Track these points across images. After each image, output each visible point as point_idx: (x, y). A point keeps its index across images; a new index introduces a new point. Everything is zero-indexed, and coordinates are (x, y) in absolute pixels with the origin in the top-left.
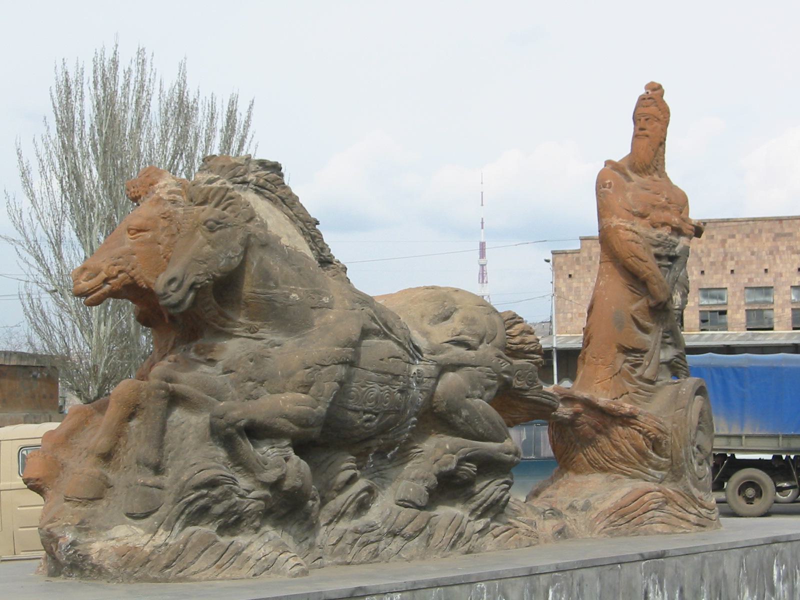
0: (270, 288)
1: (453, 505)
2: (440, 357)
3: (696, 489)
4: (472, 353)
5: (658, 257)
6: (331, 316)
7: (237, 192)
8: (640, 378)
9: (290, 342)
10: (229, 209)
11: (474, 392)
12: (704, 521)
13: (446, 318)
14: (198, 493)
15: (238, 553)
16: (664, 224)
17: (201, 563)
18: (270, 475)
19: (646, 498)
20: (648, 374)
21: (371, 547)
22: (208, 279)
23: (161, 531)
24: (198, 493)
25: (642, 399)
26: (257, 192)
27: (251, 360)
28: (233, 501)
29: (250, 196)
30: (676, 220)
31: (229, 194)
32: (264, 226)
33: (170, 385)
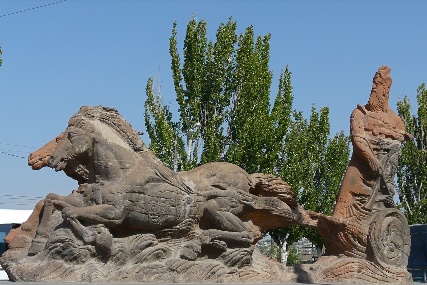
0: (99, 160)
2: (204, 192)
3: (384, 263)
4: (223, 191)
5: (375, 149)
6: (130, 172)
7: (88, 121)
8: (363, 208)
9: (106, 183)
10: (82, 128)
11: (222, 208)
12: (389, 280)
13: (214, 175)
14: (54, 245)
15: (71, 271)
16: (380, 134)
17: (54, 275)
18: (89, 238)
19: (349, 265)
20: (367, 206)
21: (157, 275)
22: (72, 157)
23: (38, 260)
24: (54, 245)
25: (363, 219)
28: (71, 249)
29: (97, 124)
30: (388, 132)
31: (83, 121)
32: (99, 134)
33: (53, 201)
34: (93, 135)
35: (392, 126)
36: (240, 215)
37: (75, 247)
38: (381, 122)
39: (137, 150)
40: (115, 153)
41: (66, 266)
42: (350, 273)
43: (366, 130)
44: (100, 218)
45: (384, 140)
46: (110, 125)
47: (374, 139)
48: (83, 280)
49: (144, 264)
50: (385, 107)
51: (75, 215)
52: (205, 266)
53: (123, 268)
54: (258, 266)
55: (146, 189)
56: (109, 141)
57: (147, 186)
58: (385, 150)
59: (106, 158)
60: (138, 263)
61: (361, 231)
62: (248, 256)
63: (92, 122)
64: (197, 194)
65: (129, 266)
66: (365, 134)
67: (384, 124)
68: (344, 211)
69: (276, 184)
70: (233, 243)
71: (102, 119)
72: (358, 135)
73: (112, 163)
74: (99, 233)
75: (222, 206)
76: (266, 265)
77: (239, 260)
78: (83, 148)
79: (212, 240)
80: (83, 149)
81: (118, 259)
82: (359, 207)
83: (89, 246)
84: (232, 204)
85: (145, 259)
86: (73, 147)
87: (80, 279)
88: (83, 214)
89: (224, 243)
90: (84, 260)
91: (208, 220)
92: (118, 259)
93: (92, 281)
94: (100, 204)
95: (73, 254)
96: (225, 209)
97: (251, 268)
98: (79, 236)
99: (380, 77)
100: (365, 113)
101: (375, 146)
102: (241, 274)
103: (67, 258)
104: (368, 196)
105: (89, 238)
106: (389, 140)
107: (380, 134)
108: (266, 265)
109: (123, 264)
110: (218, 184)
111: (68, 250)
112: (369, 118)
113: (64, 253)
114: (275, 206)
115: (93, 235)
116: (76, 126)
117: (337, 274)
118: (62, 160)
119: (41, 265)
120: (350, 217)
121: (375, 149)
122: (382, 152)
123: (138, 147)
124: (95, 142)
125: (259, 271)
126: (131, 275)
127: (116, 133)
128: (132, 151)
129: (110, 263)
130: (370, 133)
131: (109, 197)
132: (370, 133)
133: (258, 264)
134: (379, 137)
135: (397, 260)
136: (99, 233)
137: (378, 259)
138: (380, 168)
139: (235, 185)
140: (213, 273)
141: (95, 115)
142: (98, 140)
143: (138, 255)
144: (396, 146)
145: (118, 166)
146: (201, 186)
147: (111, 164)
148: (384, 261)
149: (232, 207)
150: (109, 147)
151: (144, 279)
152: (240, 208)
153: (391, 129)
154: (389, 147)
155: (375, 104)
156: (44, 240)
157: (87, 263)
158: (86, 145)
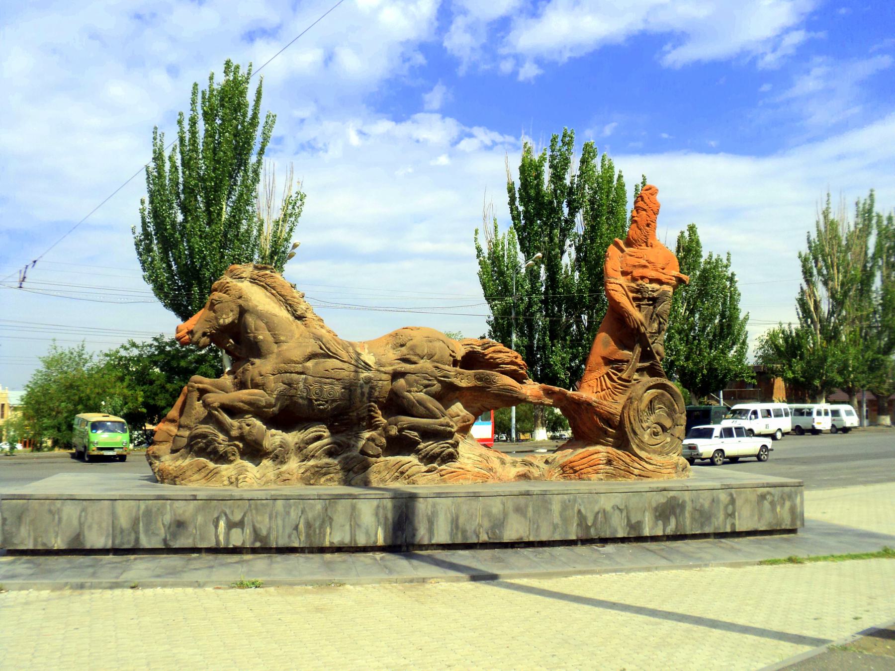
1: (409, 455)
2: (389, 369)
4: (413, 366)
5: (635, 299)
6: (284, 347)
9: (257, 361)
13: (402, 346)
15: (217, 473)
16: (642, 278)
17: (196, 477)
18: (235, 433)
19: (595, 456)
20: (624, 376)
21: (328, 477)
34: (240, 301)
35: (660, 266)
36: (437, 397)
37: (220, 444)
38: (643, 262)
39: (300, 318)
40: (266, 323)
41: (211, 465)
42: (594, 467)
43: (624, 273)
44: (246, 407)
45: (648, 285)
46: (262, 286)
47: (633, 285)
48: (232, 483)
49: (312, 462)
50: (650, 241)
51: (216, 404)
52: (392, 463)
53: (284, 468)
54: (470, 461)
55: (308, 368)
56: (260, 308)
57: (310, 364)
58: (649, 299)
59: (256, 330)
60: (303, 461)
61: (612, 411)
62: (451, 450)
63: (240, 284)
64: (378, 370)
65: (293, 465)
66: (622, 280)
67: (648, 264)
68: (593, 383)
69: (494, 352)
70: (429, 434)
71: (253, 281)
72: (612, 280)
73: (263, 335)
74: (248, 425)
75: (411, 385)
76: (480, 459)
77: (439, 455)
78: (228, 319)
79: (401, 430)
80: (228, 320)
81: (277, 457)
82: (615, 378)
83: (237, 443)
84: (426, 382)
85: (313, 456)
86: (217, 319)
87: (226, 482)
88: (226, 402)
89: (416, 434)
90: (232, 458)
91: (396, 405)
92: (277, 457)
93: (239, 485)
95: (217, 452)
96: (415, 389)
97: (457, 464)
98: (223, 428)
99: (642, 200)
100: (622, 251)
101: (635, 295)
102: (443, 473)
103: (212, 456)
104: (628, 361)
105: (235, 433)
106: (656, 286)
107: (642, 278)
108: (480, 459)
109: (283, 462)
110: (408, 356)
111: (212, 447)
112: (628, 257)
113: (209, 450)
114: (488, 381)
117: (577, 468)
118: (204, 334)
119: (184, 464)
120: (603, 390)
121: (635, 299)
122: (645, 302)
123: (299, 313)
124: (243, 311)
125: (469, 467)
126: (295, 477)
127: (269, 297)
128: (291, 318)
129: (266, 462)
131: (259, 379)
132: (629, 277)
133: (468, 458)
134: (640, 282)
135: (663, 447)
136: (248, 425)
137: (634, 447)
138: (642, 324)
139: (430, 357)
140: (402, 473)
141: (244, 275)
142: (246, 308)
143: (304, 451)
144: (664, 293)
145: (271, 339)
146: (384, 360)
147: (261, 337)
148: (642, 449)
149: (426, 386)
150: (260, 316)
151: (312, 482)
152: (437, 387)
153: (657, 270)
154: (655, 294)
155: (635, 237)
156: (187, 433)
157: (235, 463)
158: (231, 314)
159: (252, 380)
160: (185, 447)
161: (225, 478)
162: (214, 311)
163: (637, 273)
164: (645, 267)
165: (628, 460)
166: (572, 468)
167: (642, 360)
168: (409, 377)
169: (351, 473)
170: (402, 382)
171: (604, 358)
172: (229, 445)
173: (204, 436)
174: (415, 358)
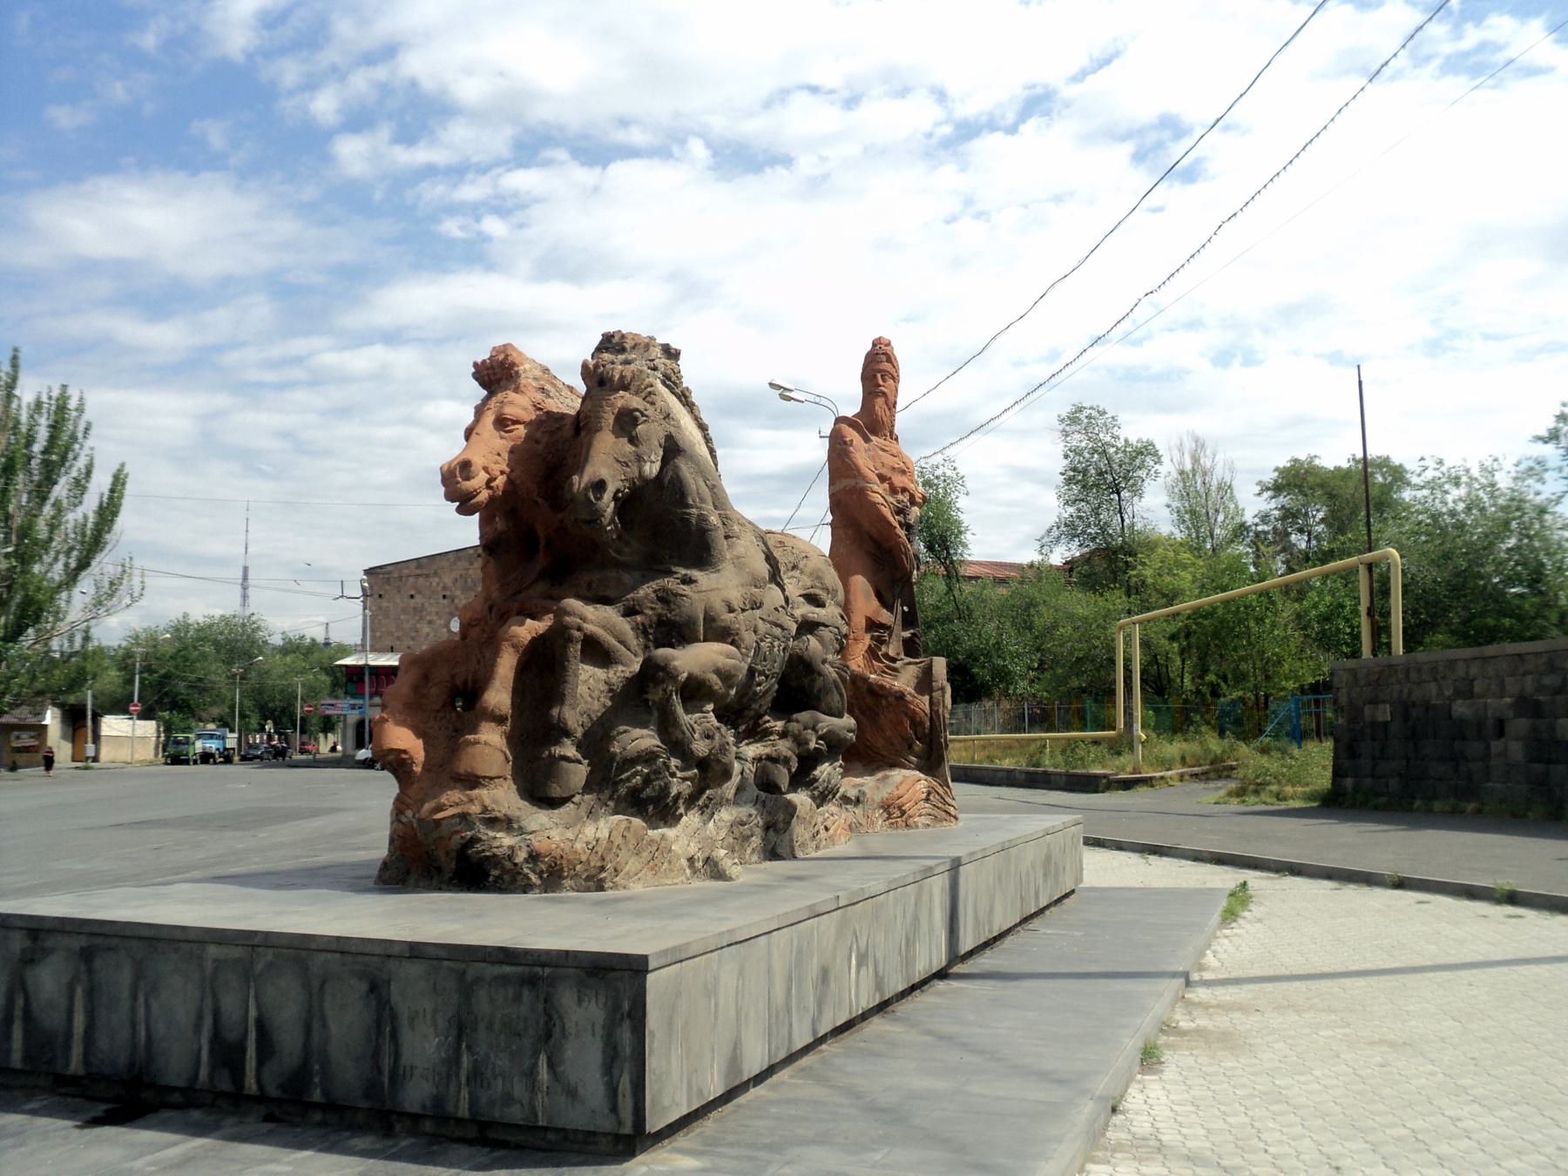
0: (688, 506)
2: (798, 613)
20: (891, 653)
26: (664, 383)
27: (661, 599)
32: (678, 427)
43: (882, 478)
72: (875, 488)
94: (698, 641)
100: (867, 440)
107: (904, 490)
110: (818, 591)
113: (648, 791)
115: (708, 737)
116: (637, 393)
130: (886, 485)
134: (900, 497)
159: (710, 619)
160: (588, 788)
161: (684, 862)
162: (633, 440)
163: (899, 481)
164: (903, 472)
165: (940, 791)
166: (900, 808)
167: (905, 627)
168: (823, 632)
169: (771, 832)
170: (813, 642)
171: (868, 619)
172: (685, 779)
173: (648, 757)
174: (823, 595)
